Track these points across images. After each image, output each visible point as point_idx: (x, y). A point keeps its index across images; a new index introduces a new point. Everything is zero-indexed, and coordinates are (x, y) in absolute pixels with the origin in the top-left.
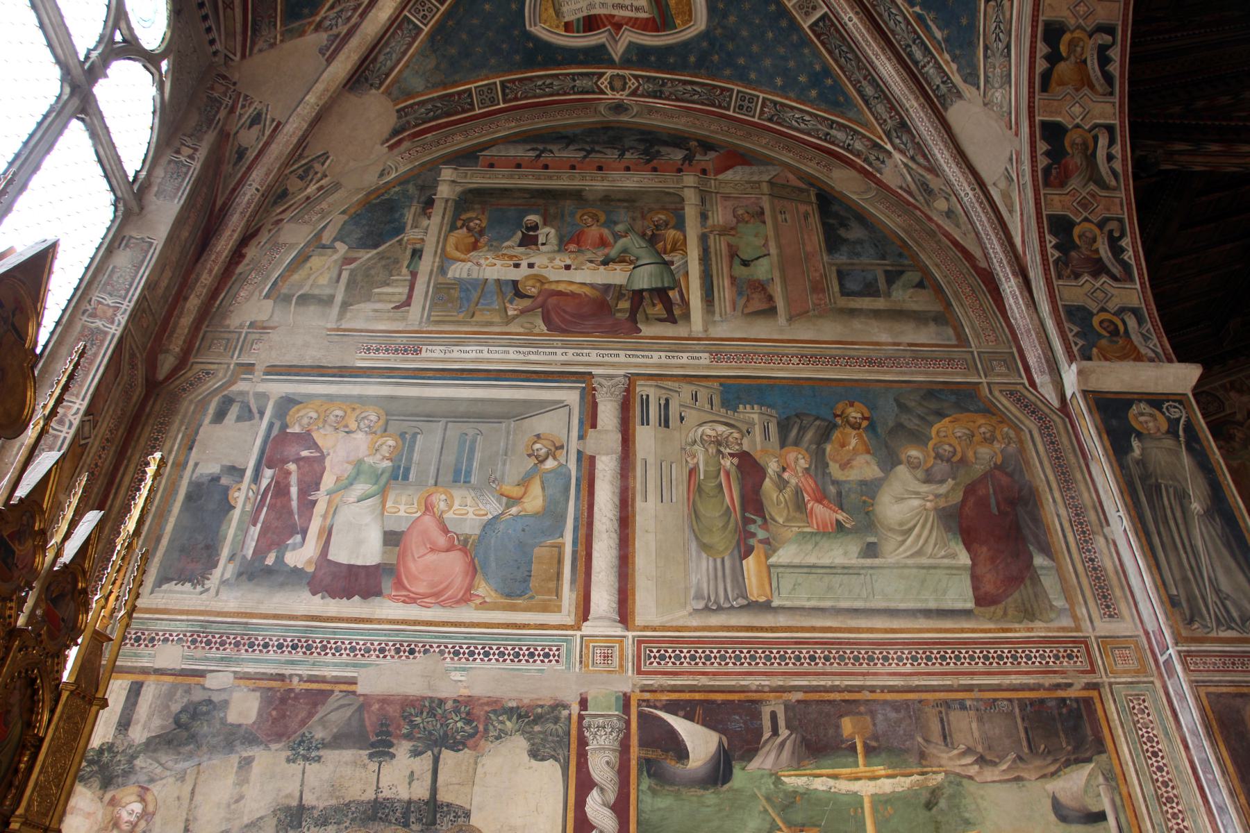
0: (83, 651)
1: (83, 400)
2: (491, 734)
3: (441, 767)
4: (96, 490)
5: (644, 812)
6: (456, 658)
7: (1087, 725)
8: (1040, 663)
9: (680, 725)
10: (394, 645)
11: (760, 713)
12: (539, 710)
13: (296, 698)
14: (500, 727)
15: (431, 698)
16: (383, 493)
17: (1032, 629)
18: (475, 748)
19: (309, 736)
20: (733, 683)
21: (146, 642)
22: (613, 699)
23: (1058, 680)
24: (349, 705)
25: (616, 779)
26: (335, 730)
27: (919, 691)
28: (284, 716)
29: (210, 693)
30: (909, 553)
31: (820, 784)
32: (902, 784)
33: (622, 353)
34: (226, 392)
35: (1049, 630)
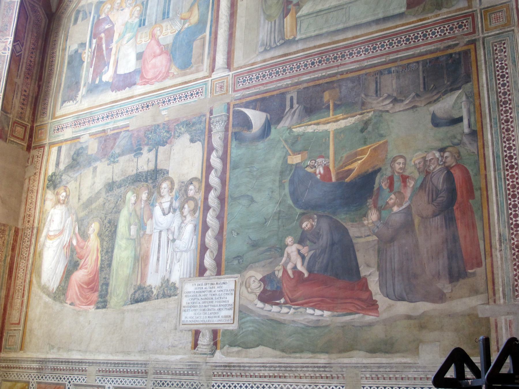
1: (11, 36)
2: (176, 135)
4: (35, 72)
7: (463, 67)
8: (440, 35)
9: (250, 113)
11: (285, 99)
15: (155, 125)
16: (135, 36)
17: (439, 15)
20: (275, 86)
23: (451, 43)
25: (222, 144)
27: (366, 69)
28: (106, 147)
31: (310, 129)
32: (350, 121)
34: (77, 8)
35: (450, 12)
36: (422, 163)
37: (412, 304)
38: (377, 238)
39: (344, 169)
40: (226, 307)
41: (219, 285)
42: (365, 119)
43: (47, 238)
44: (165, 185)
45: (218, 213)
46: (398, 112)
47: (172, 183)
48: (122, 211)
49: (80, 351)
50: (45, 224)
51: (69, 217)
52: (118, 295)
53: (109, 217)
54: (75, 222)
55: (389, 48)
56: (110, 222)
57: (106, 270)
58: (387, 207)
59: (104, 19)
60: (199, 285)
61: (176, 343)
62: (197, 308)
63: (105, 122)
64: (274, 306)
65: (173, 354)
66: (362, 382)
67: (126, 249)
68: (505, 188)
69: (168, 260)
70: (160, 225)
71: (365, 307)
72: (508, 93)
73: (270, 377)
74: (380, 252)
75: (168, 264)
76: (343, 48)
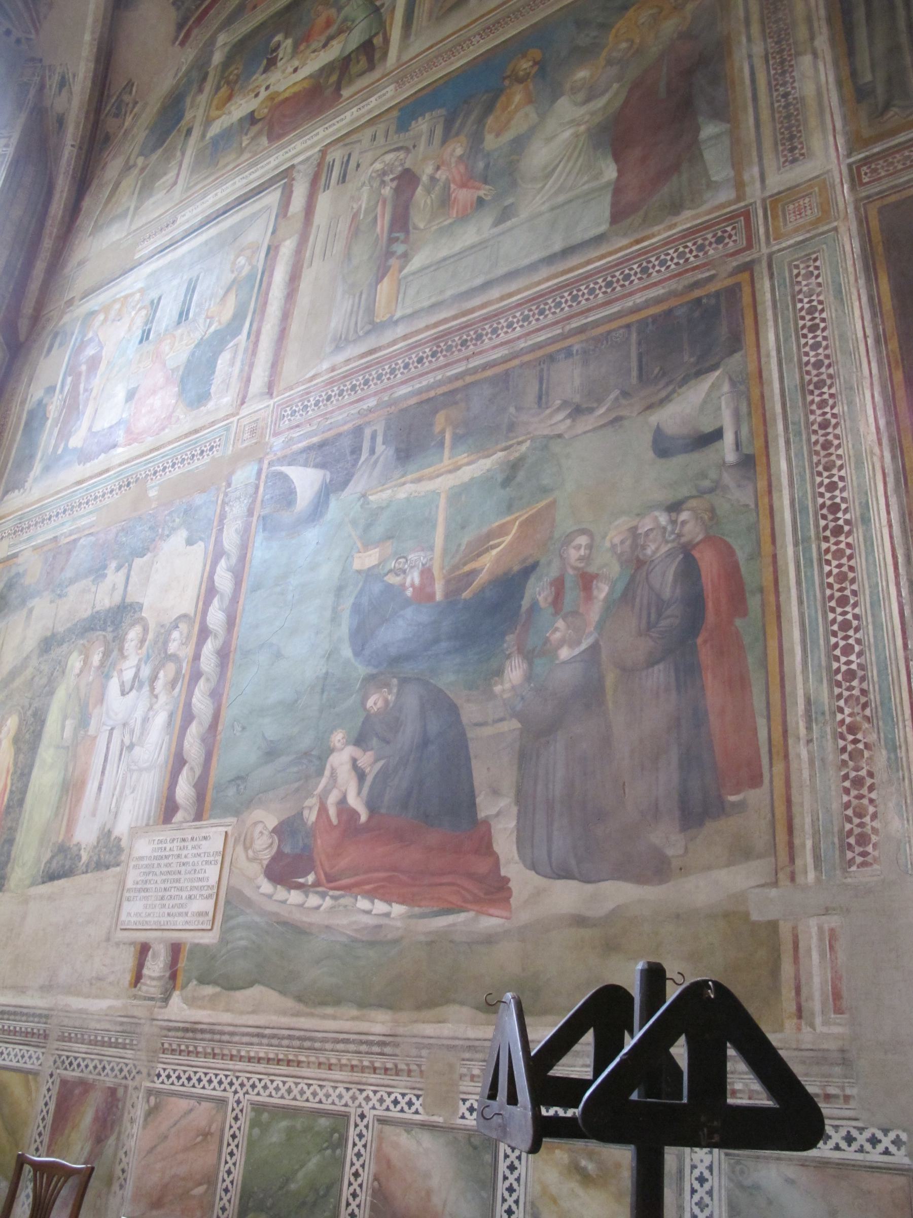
14: (170, 524)
30: (545, 198)
32: (484, 465)
33: (321, 129)
36: (628, 543)
37: (589, 888)
38: (519, 725)
39: (461, 572)
40: (203, 892)
41: (195, 843)
42: (512, 458)
44: (133, 634)
45: (213, 684)
46: (581, 435)
53: (36, 704)
55: (570, 306)
56: (35, 715)
58: (547, 651)
59: (91, 340)
62: (150, 894)
64: (293, 892)
65: (97, 997)
66: (463, 1089)
68: (822, 584)
69: (115, 789)
71: (481, 895)
72: (826, 362)
73: (269, 1060)
74: (524, 758)
76: (481, 321)
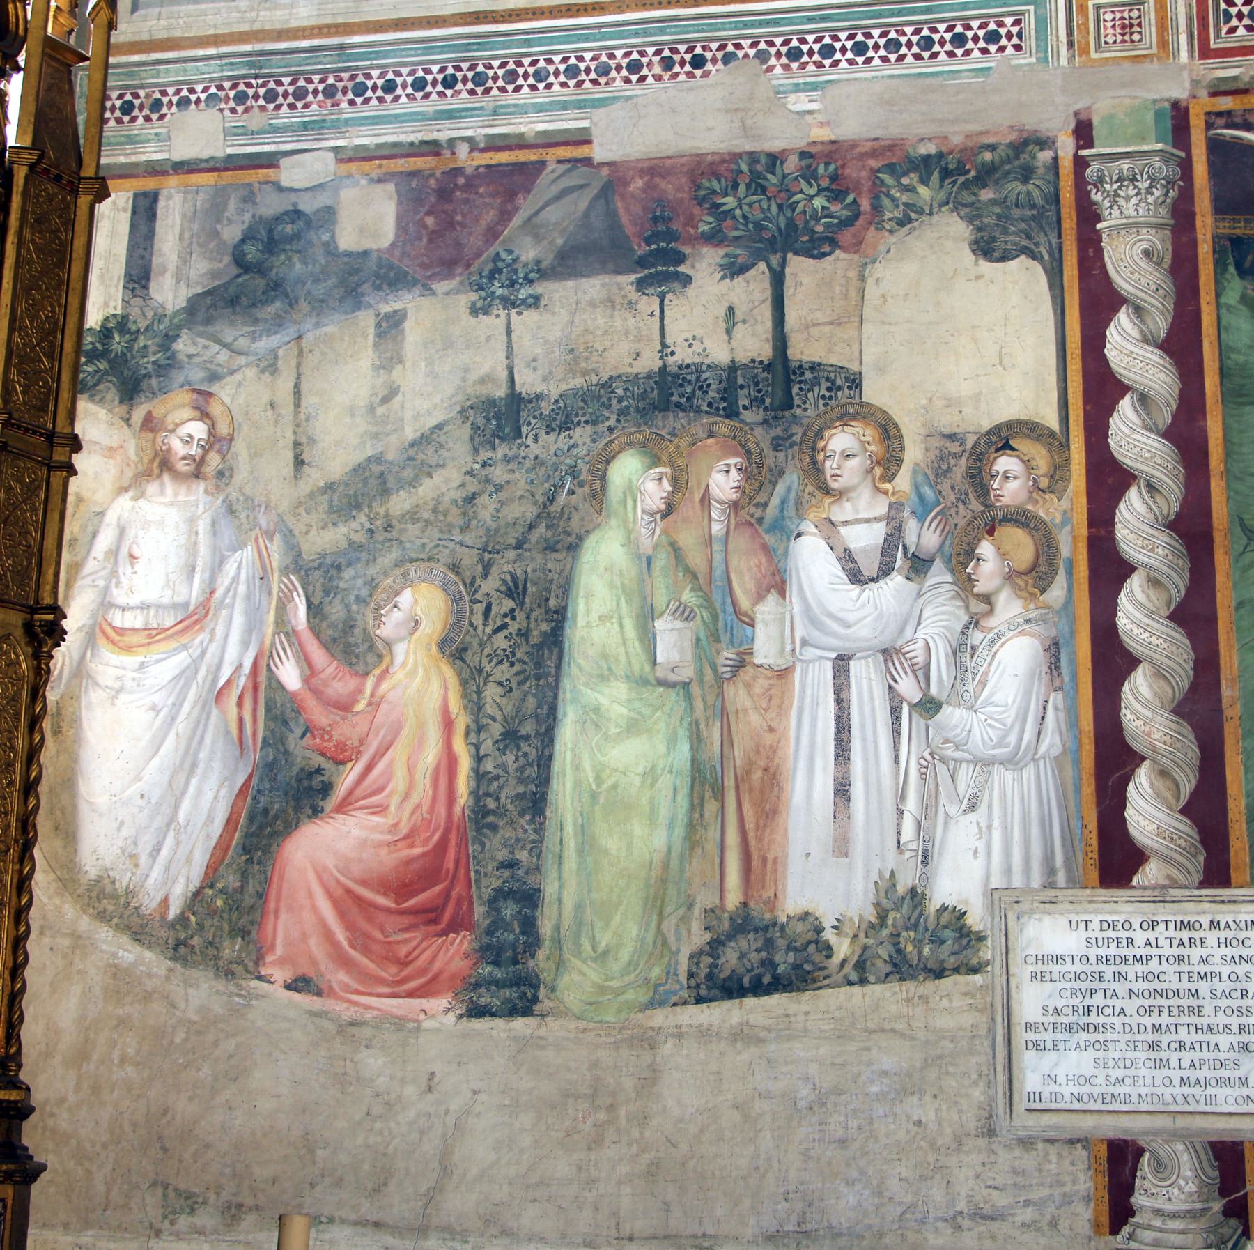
0: (34, 80)
2: (888, 215)
3: (789, 291)
5: (1233, 350)
6: (795, 65)
10: (658, 52)
12: (988, 156)
13: (470, 185)
14: (905, 198)
15: (751, 153)
18: (856, 246)
19: (509, 259)
21: (146, 112)
22: (1150, 117)
24: (582, 187)
25: (1168, 286)
26: (560, 241)
28: (451, 225)
29: (293, 197)
41: (1223, 934)
43: (101, 641)
47: (889, 432)
48: (590, 543)
49: (377, 1225)
50: (76, 567)
51: (240, 546)
52: (603, 956)
53: (505, 566)
54: (285, 571)
56: (514, 590)
57: (511, 823)
60: (1112, 925)
61: (1001, 1200)
62: (1109, 1037)
63: (434, 104)
67: (633, 727)
69: (903, 797)
70: (842, 631)
75: (906, 815)
